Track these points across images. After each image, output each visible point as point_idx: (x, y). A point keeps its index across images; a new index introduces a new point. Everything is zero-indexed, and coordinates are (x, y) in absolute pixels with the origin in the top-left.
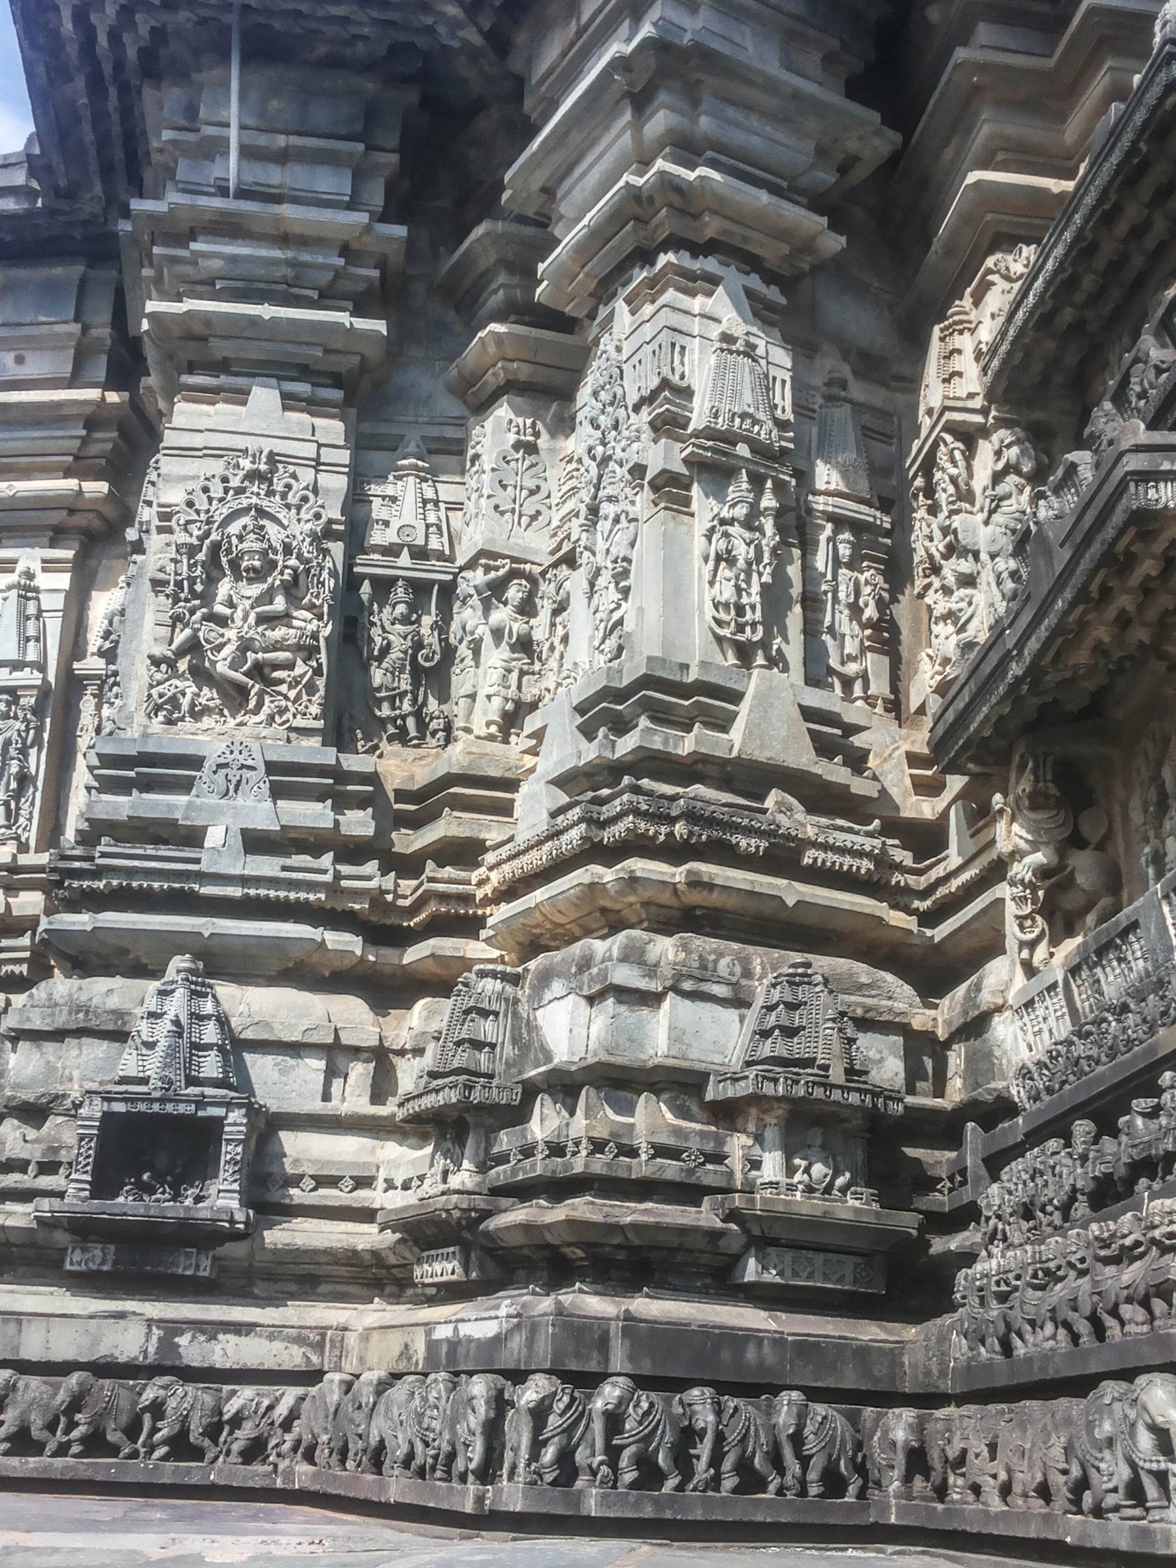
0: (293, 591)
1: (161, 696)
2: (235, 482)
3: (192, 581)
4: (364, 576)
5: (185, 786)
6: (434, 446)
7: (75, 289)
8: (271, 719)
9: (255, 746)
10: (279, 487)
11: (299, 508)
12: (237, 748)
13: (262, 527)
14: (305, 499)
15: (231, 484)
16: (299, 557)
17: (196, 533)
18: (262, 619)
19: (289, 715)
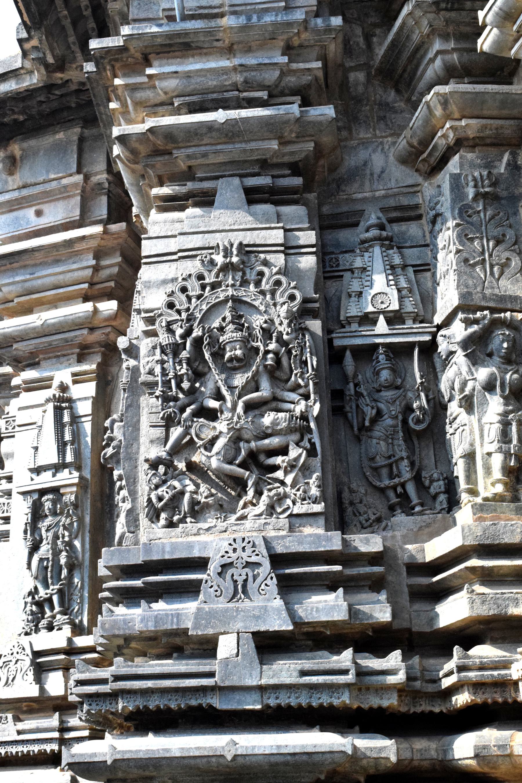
0: (278, 374)
1: (160, 499)
2: (210, 279)
3: (179, 379)
4: (344, 348)
5: (192, 590)
6: (394, 214)
7: (75, 148)
8: (271, 510)
9: (260, 542)
10: (251, 276)
11: (273, 293)
12: (239, 545)
13: (241, 317)
14: (278, 283)
15: (207, 281)
16: (280, 340)
17: (179, 332)
18: (249, 407)
19: (289, 502)
